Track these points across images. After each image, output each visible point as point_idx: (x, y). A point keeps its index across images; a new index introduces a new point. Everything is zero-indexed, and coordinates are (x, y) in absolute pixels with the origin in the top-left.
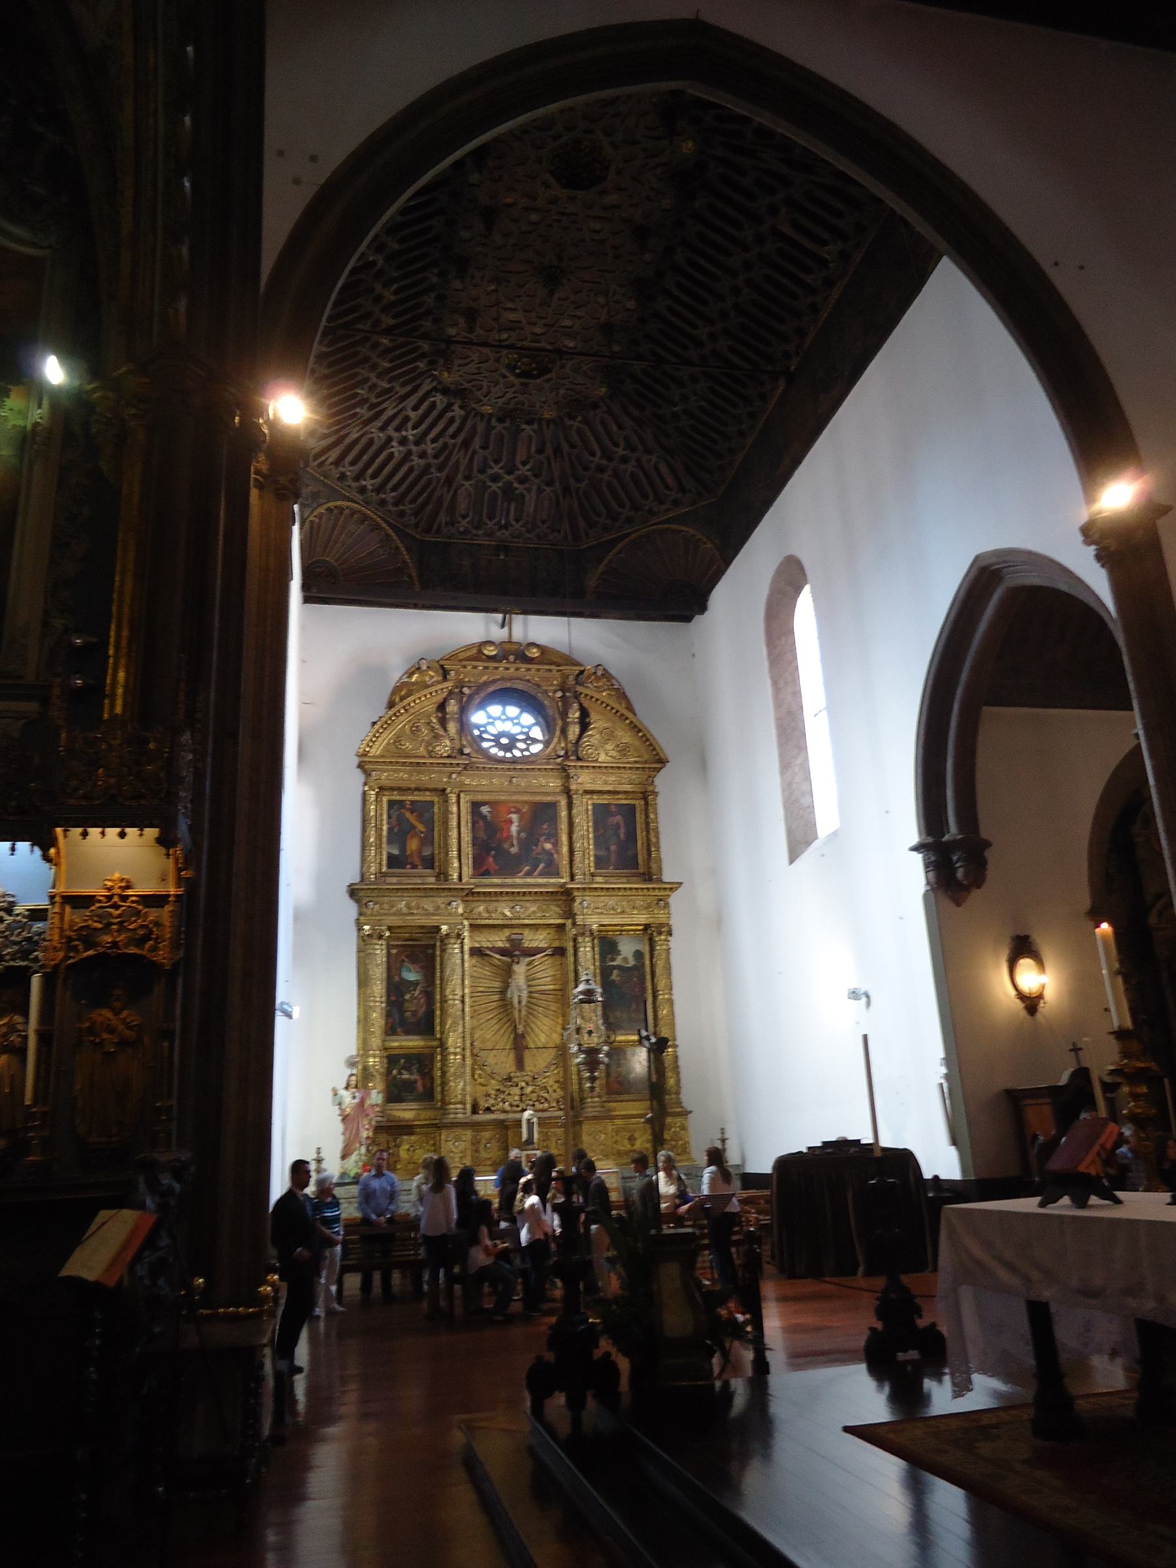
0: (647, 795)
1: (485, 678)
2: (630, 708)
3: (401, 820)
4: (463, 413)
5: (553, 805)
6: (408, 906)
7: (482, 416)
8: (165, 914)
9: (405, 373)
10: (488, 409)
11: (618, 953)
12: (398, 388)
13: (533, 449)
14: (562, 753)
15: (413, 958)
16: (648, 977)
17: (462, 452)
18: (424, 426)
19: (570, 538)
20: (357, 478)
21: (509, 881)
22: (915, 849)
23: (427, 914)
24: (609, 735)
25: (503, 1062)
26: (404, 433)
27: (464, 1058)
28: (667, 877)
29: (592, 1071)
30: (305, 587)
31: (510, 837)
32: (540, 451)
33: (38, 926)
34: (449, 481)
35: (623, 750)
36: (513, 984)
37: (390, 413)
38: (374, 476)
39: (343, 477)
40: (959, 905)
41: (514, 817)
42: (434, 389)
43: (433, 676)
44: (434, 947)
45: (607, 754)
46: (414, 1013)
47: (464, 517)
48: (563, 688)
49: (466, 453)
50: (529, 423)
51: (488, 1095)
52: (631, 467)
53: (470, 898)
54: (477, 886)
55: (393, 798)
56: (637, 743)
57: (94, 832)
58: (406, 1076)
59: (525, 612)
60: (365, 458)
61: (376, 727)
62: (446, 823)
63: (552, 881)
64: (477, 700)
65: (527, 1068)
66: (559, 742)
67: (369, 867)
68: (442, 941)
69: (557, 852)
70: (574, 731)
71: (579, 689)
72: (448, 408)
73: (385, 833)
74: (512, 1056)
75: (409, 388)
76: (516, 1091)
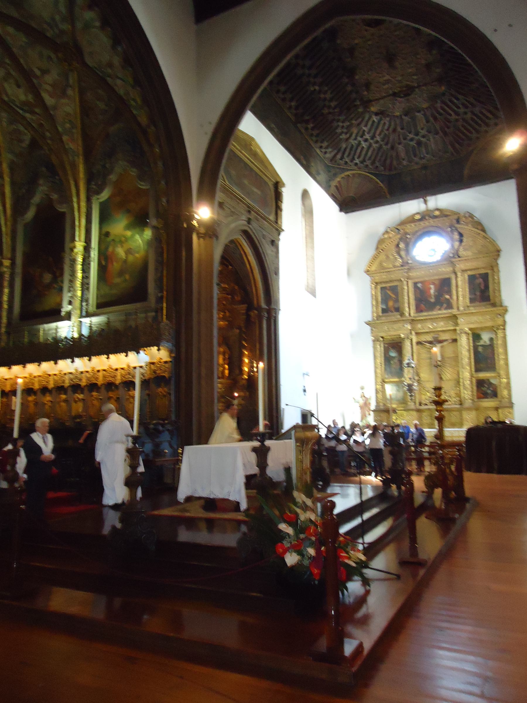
0: (494, 267)
7: (397, 116)
10: (398, 114)
19: (454, 153)
21: (430, 313)
29: (410, 393)
31: (430, 296)
32: (428, 121)
38: (359, 157)
39: (346, 163)
44: (401, 343)
50: (419, 112)
52: (469, 116)
60: (353, 153)
63: (450, 311)
64: (413, 240)
70: (457, 244)
75: (360, 120)
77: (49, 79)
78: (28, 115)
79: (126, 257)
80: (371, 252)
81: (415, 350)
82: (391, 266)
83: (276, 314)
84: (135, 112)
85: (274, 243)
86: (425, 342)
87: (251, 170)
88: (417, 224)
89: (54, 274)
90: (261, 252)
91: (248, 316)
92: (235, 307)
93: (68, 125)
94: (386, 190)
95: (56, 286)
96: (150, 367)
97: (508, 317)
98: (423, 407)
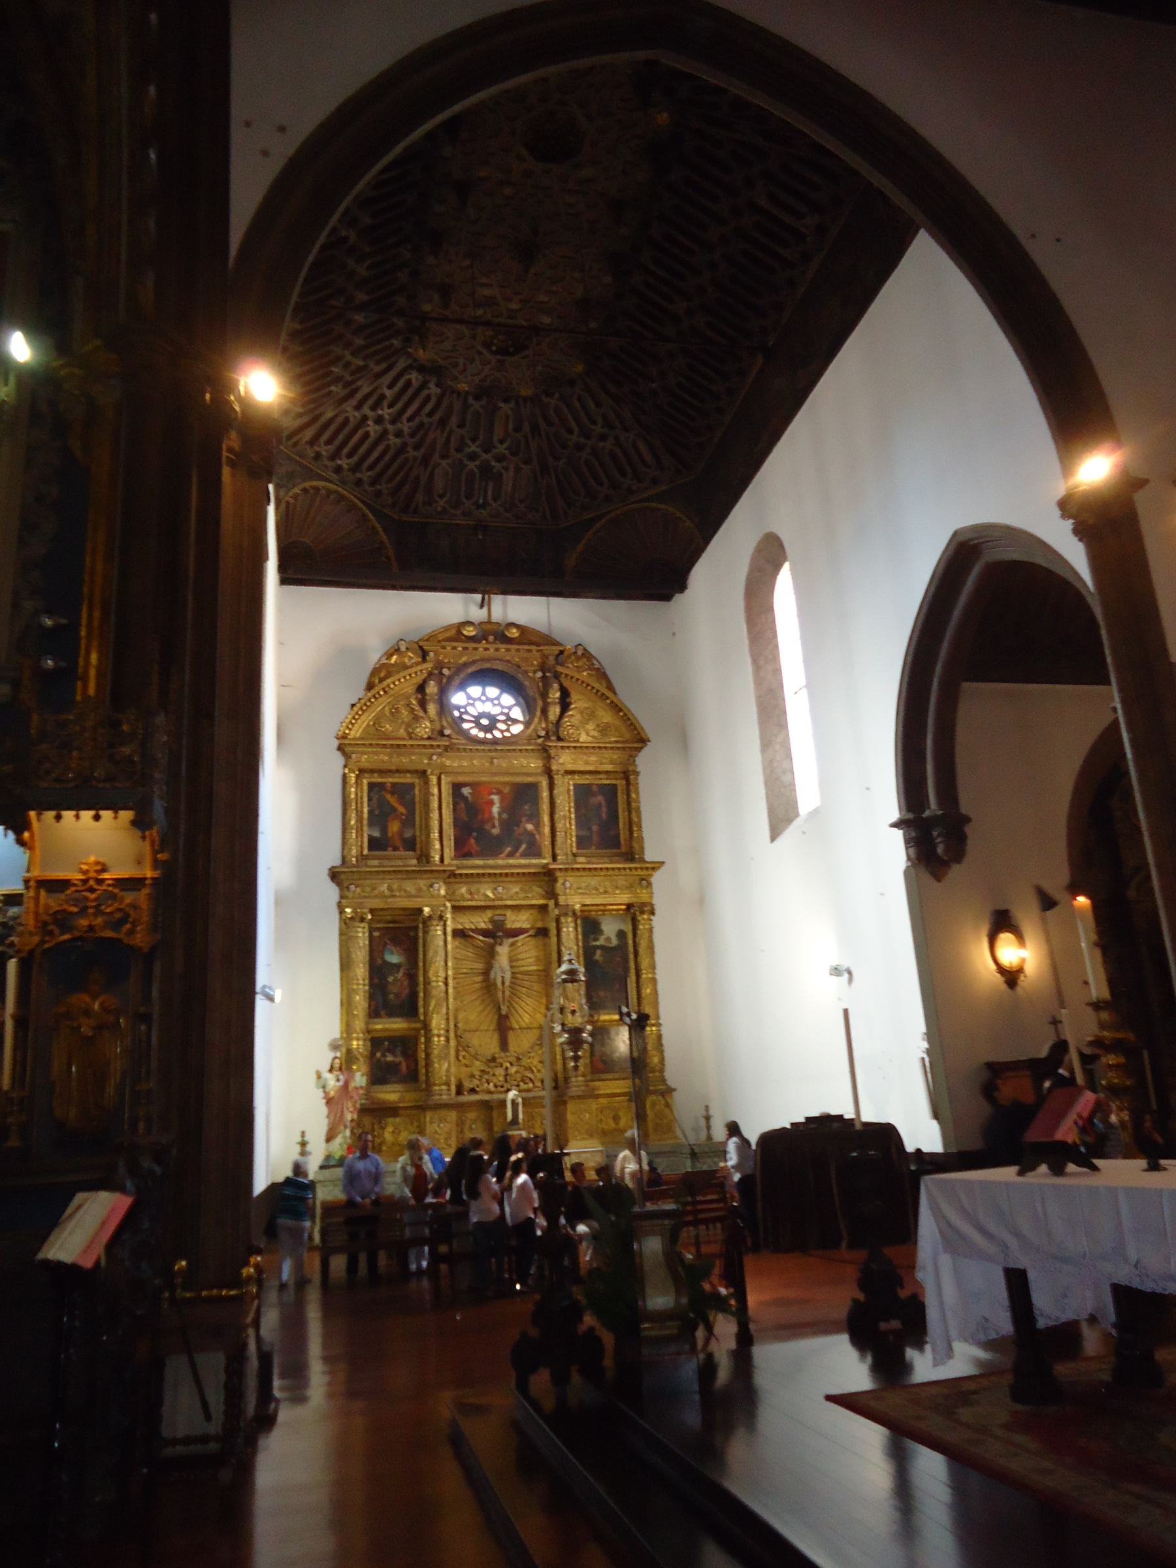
0: (628, 775)
1: (464, 659)
2: (610, 687)
3: (382, 802)
4: (438, 391)
5: (533, 787)
6: (390, 889)
7: (459, 394)
8: (142, 897)
10: (463, 386)
11: (601, 932)
12: (372, 365)
13: (511, 427)
14: (543, 733)
15: (396, 941)
16: (631, 956)
18: (400, 405)
20: (332, 458)
21: (491, 862)
22: (895, 825)
23: (411, 896)
24: (591, 715)
25: (487, 1043)
26: (380, 412)
27: (448, 1040)
28: (650, 855)
29: (576, 1050)
30: (282, 568)
31: (492, 818)
32: (517, 429)
33: (13, 911)
34: (426, 460)
35: (604, 730)
36: (496, 966)
37: (366, 390)
38: (350, 456)
39: (318, 456)
40: (939, 881)
41: (495, 798)
42: (408, 368)
43: (412, 657)
44: (416, 928)
45: (588, 734)
46: (397, 995)
47: (441, 496)
48: (543, 668)
49: (443, 432)
50: (506, 401)
51: (473, 1076)
52: (609, 445)
53: (452, 880)
54: (458, 867)
55: (373, 780)
56: (617, 723)
57: (68, 815)
58: (390, 1058)
59: (505, 592)
60: (341, 437)
61: (355, 709)
62: (426, 804)
63: (534, 861)
64: (457, 681)
65: (511, 1048)
66: (540, 722)
67: (350, 849)
68: (424, 923)
69: (539, 833)
71: (559, 669)
72: (424, 385)
73: (366, 815)
74: (496, 1036)
75: (384, 365)
76: (500, 1072)
86: (472, 930)
88: (471, 645)
94: (391, 553)
97: (661, 888)
98: (467, 1098)
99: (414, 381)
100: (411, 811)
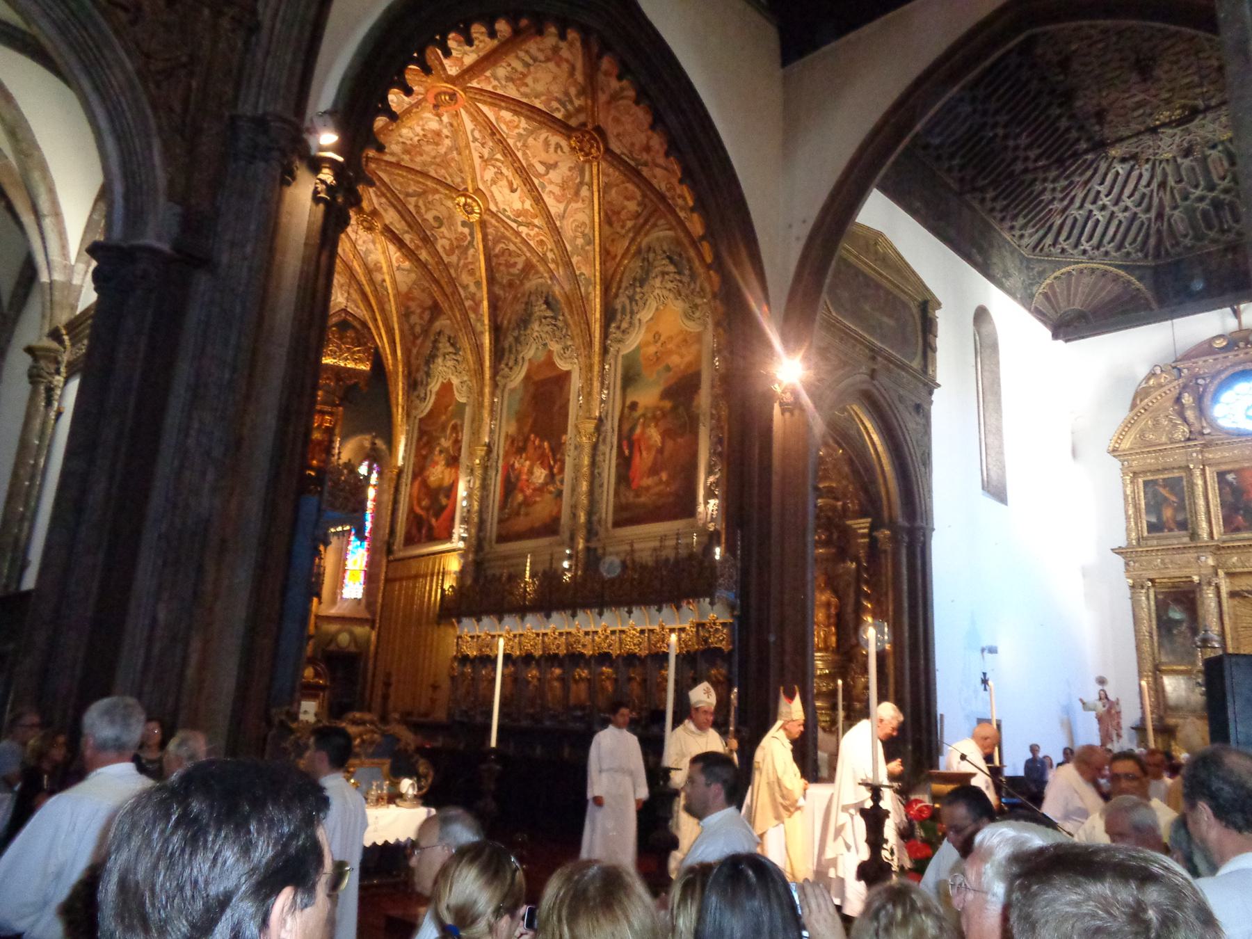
3: (1155, 494)
6: (1163, 562)
9: (1077, 169)
17: (1161, 193)
18: (1116, 190)
37: (1081, 195)
38: (1090, 238)
39: (1063, 251)
44: (1194, 592)
50: (1214, 147)
60: (1076, 232)
64: (1212, 388)
73: (1143, 506)
75: (1089, 173)
77: (554, 175)
78: (521, 229)
79: (663, 442)
80: (1123, 413)
81: (1225, 608)
82: (1164, 439)
83: (924, 535)
84: (682, 215)
85: (922, 410)
87: (878, 286)
88: (1220, 356)
89: (551, 468)
90: (896, 424)
91: (873, 542)
92: (849, 522)
93: (580, 241)
94: (1149, 295)
95: (551, 488)
96: (697, 632)
99: (1121, 171)
100: (1183, 500)
